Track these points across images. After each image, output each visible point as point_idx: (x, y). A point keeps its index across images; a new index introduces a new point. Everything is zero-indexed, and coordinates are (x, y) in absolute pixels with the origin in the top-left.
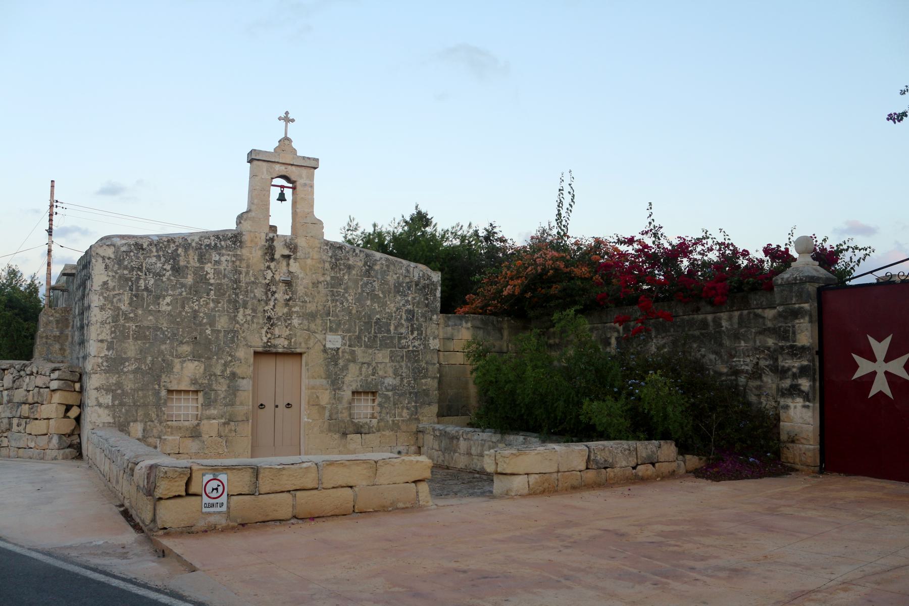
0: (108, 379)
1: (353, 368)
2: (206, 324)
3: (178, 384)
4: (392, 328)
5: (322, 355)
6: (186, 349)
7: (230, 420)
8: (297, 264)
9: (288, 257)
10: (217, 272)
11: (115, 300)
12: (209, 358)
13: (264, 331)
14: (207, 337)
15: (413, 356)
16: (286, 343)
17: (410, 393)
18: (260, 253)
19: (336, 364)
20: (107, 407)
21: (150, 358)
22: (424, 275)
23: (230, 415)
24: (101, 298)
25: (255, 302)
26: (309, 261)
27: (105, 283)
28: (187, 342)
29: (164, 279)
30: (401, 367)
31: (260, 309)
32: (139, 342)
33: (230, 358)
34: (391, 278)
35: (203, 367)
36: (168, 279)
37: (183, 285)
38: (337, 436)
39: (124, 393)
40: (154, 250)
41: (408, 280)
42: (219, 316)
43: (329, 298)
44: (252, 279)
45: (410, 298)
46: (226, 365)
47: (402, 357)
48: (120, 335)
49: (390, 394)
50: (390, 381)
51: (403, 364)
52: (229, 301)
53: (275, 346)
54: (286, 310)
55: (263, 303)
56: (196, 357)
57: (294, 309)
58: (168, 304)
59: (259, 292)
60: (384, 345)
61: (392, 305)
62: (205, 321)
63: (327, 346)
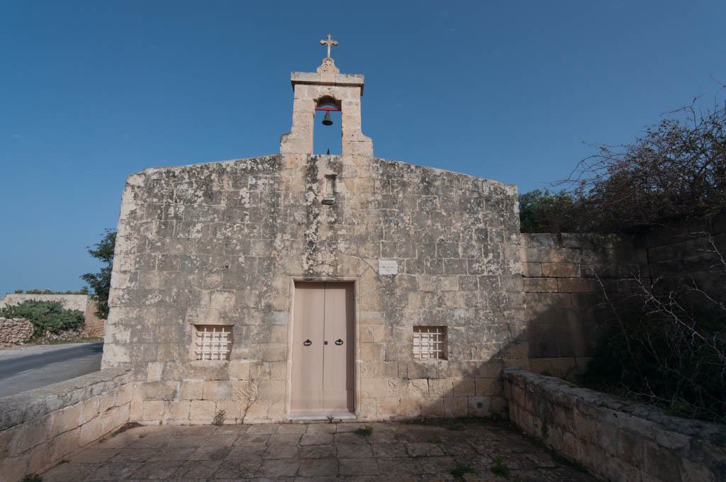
0: (128, 313)
1: (414, 299)
2: (240, 251)
3: (206, 318)
4: (460, 250)
5: (375, 284)
6: (215, 278)
7: (263, 361)
8: (343, 184)
9: (332, 178)
10: (253, 196)
11: (142, 229)
12: (242, 289)
13: (304, 258)
14: (239, 266)
15: (489, 282)
16: (331, 270)
17: (489, 328)
18: (300, 174)
19: (392, 294)
20: (124, 344)
21: (175, 290)
22: (496, 189)
23: (264, 354)
24: (128, 227)
25: (295, 226)
26: (357, 180)
27: (133, 212)
28: (217, 272)
29: (195, 206)
30: (474, 296)
31: (301, 233)
32: (165, 272)
33: (265, 288)
34: (455, 195)
35: (234, 299)
36: (200, 205)
37: (216, 211)
38: (396, 381)
39: (145, 329)
40: (186, 177)
41: (476, 195)
42: (254, 243)
43: (381, 219)
44: (292, 202)
45: (480, 216)
46: (260, 296)
47: (475, 284)
48: (145, 264)
49: (463, 329)
50: (461, 313)
51: (478, 292)
52: (266, 226)
53: (318, 274)
54: (330, 233)
55: (303, 226)
56: (226, 288)
57: (339, 233)
58: (198, 232)
59: (299, 215)
60: (450, 271)
61: (459, 224)
62: (238, 248)
63: (381, 273)
